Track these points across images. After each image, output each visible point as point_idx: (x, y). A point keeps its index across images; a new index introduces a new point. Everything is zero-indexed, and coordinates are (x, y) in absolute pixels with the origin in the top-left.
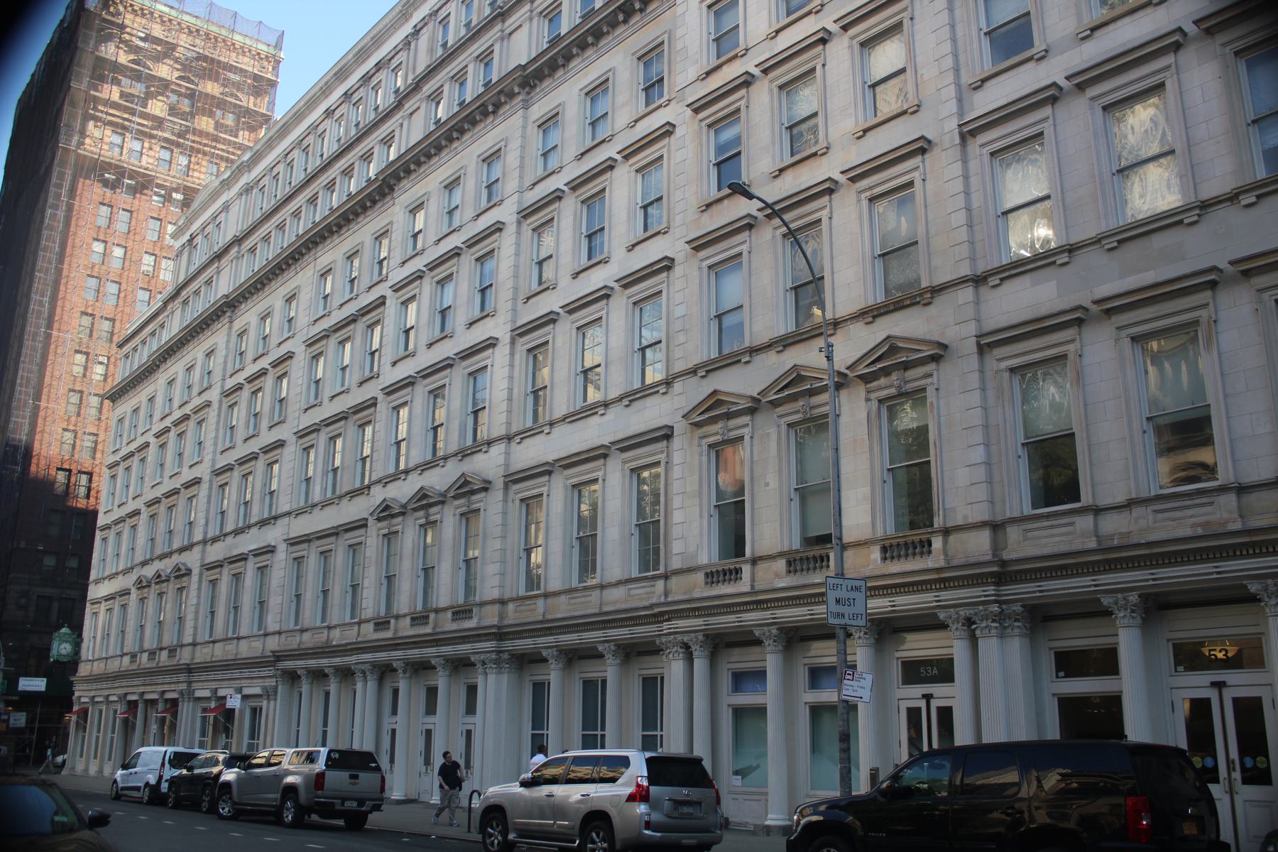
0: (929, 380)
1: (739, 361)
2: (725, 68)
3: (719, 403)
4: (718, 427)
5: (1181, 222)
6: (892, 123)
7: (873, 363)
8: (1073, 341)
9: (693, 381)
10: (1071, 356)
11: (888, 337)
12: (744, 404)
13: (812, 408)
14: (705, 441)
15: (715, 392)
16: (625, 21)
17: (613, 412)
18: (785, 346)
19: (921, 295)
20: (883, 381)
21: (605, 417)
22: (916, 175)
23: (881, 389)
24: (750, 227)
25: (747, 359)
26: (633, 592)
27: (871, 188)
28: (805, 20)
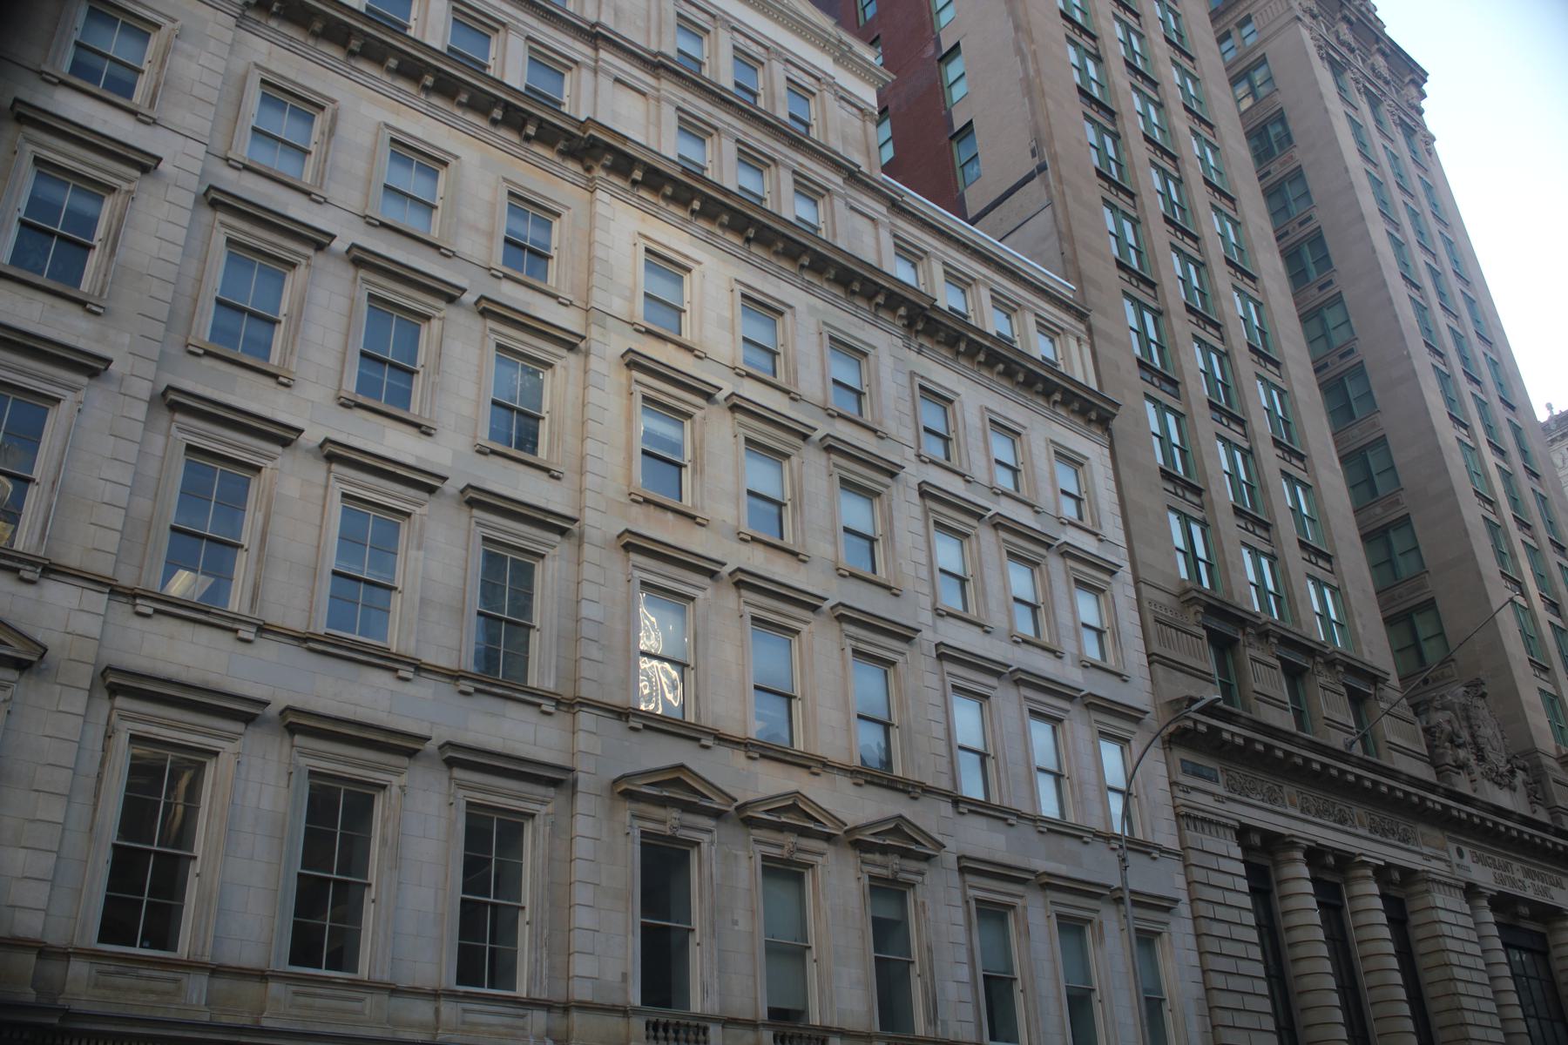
0: (919, 878)
1: (698, 740)
2: (670, 346)
3: (677, 783)
4: (673, 815)
5: (1081, 837)
6: (874, 588)
7: (917, 842)
8: (1021, 897)
9: (617, 726)
10: (1019, 910)
11: (901, 817)
12: (717, 803)
13: (800, 850)
14: (638, 823)
15: (681, 767)
16: (494, 122)
17: (269, 649)
18: (763, 756)
19: (914, 786)
20: (877, 857)
21: (407, 687)
22: (900, 659)
23: (874, 864)
24: (712, 574)
25: (709, 743)
26: (471, 1017)
27: (857, 640)
28: (778, 393)
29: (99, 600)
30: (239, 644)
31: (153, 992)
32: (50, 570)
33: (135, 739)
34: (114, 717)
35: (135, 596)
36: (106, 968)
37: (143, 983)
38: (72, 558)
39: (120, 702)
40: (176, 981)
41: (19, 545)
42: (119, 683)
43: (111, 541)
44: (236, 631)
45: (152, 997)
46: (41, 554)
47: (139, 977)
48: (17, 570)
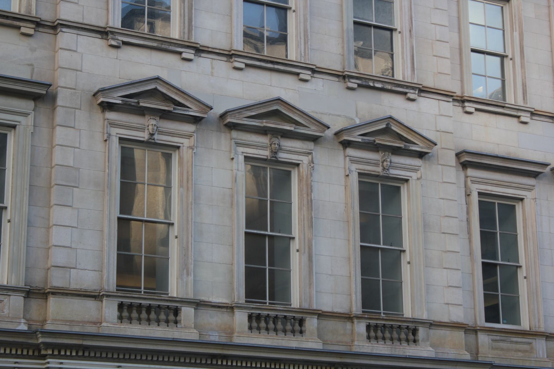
29: (449, 107)
30: (521, 125)
31: (520, 351)
32: (423, 91)
33: (480, 194)
34: (469, 183)
35: (463, 101)
36: (495, 338)
37: (514, 346)
38: (429, 82)
39: (471, 172)
40: (530, 343)
41: (399, 76)
42: (468, 161)
43: (446, 66)
44: (518, 117)
45: (520, 354)
46: (415, 81)
47: (512, 342)
48: (405, 94)
